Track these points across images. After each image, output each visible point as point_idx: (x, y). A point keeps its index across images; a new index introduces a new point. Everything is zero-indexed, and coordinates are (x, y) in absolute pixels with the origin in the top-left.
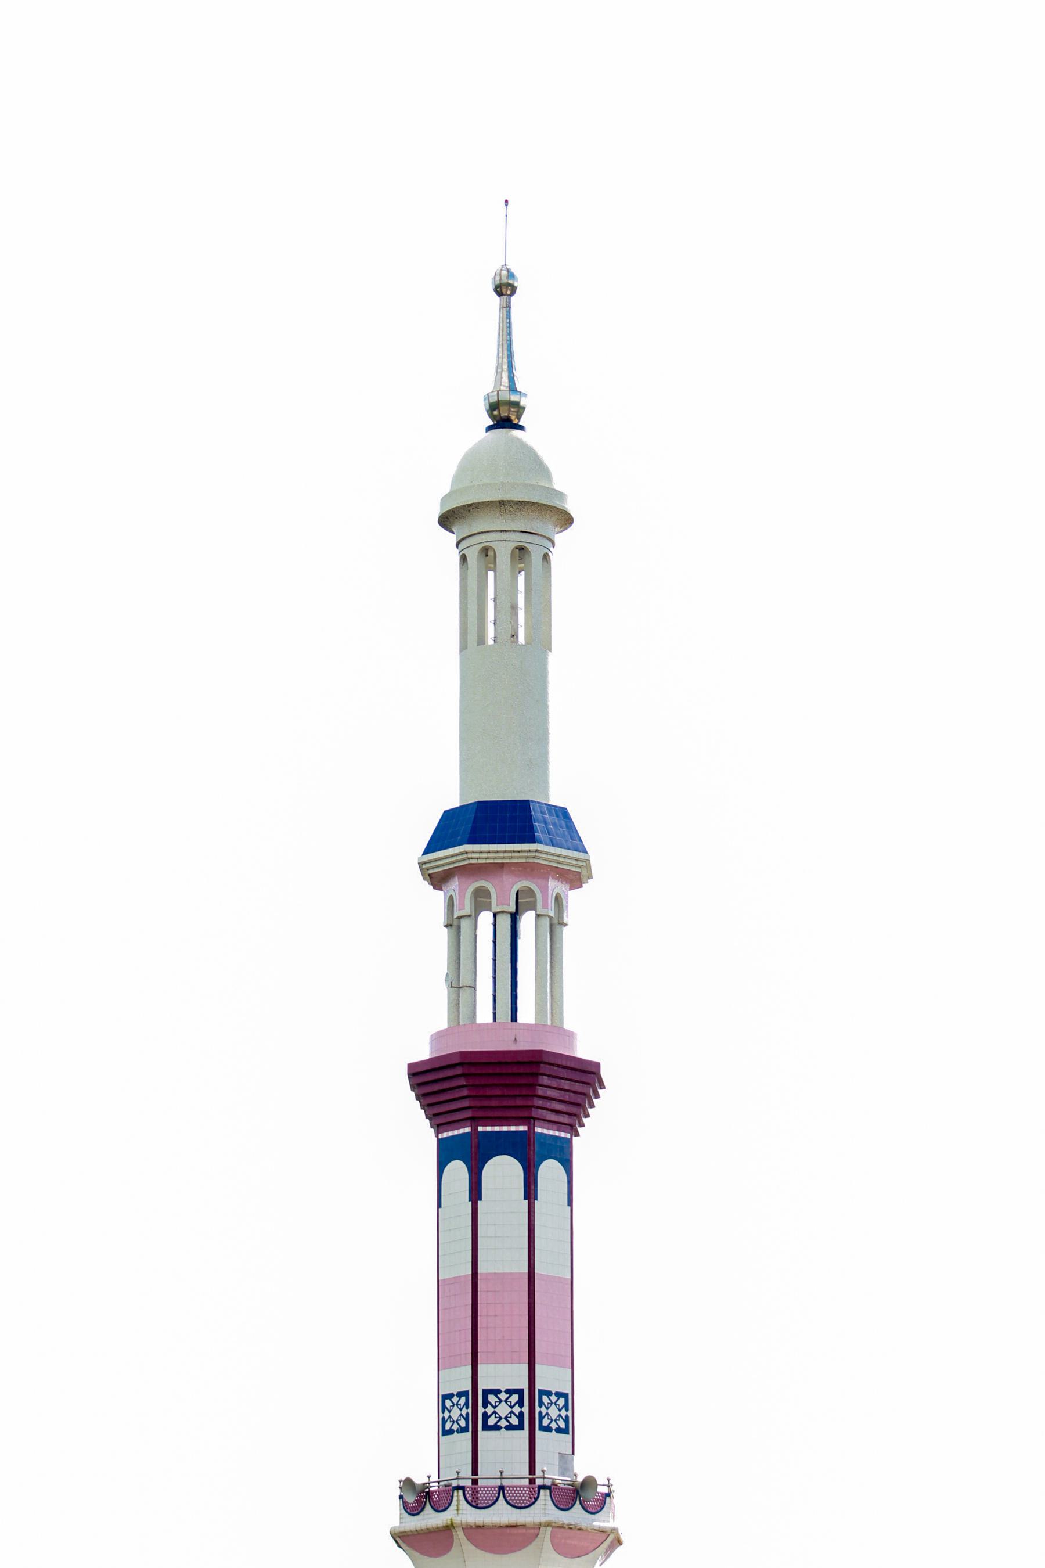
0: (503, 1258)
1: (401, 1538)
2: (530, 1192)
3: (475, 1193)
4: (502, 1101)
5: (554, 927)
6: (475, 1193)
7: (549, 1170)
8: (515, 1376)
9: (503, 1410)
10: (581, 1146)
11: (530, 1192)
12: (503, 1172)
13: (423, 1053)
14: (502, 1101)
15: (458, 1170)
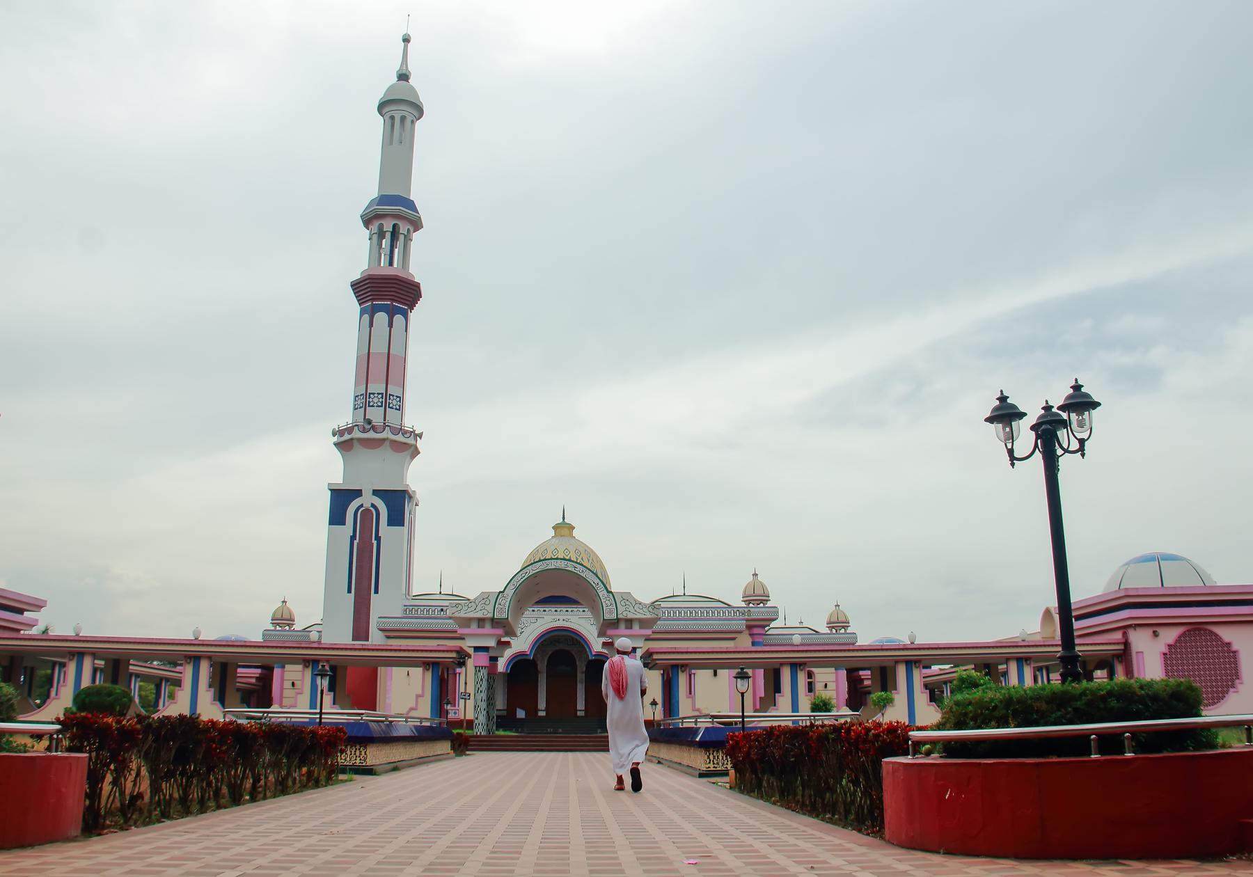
0: (379, 347)
1: (336, 444)
2: (391, 325)
3: (371, 325)
4: (387, 294)
5: (408, 239)
6: (371, 325)
7: (398, 318)
8: (377, 387)
9: (376, 400)
10: (413, 315)
11: (391, 325)
12: (381, 317)
13: (357, 276)
14: (387, 294)
15: (366, 317)
